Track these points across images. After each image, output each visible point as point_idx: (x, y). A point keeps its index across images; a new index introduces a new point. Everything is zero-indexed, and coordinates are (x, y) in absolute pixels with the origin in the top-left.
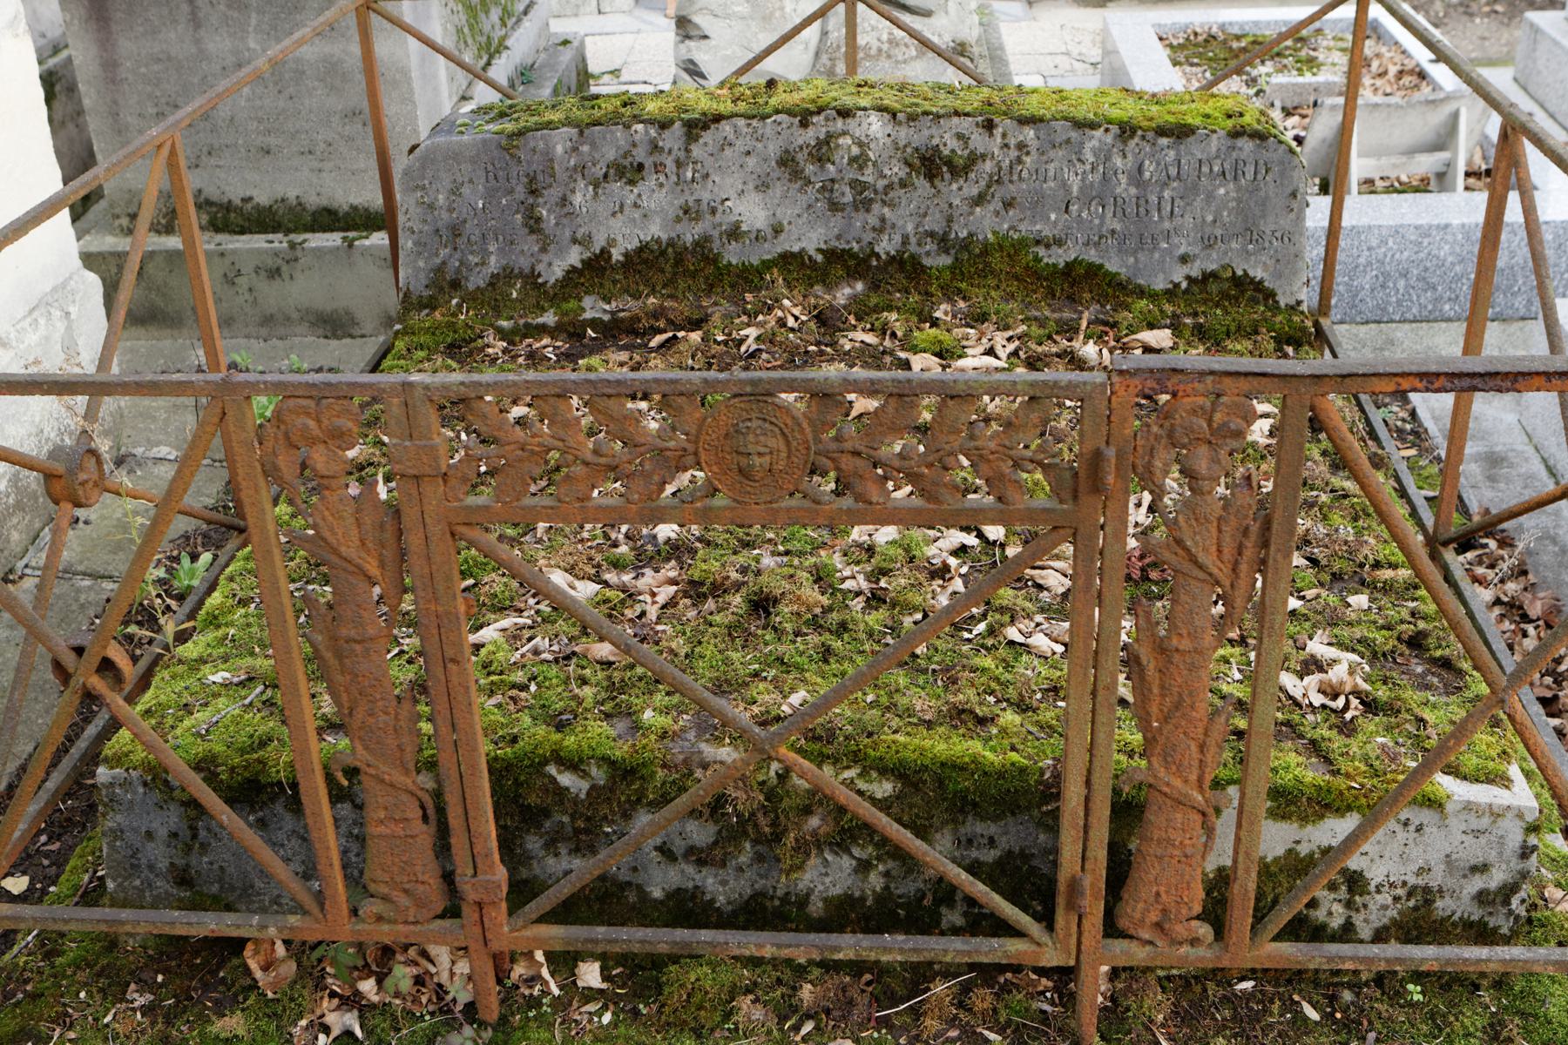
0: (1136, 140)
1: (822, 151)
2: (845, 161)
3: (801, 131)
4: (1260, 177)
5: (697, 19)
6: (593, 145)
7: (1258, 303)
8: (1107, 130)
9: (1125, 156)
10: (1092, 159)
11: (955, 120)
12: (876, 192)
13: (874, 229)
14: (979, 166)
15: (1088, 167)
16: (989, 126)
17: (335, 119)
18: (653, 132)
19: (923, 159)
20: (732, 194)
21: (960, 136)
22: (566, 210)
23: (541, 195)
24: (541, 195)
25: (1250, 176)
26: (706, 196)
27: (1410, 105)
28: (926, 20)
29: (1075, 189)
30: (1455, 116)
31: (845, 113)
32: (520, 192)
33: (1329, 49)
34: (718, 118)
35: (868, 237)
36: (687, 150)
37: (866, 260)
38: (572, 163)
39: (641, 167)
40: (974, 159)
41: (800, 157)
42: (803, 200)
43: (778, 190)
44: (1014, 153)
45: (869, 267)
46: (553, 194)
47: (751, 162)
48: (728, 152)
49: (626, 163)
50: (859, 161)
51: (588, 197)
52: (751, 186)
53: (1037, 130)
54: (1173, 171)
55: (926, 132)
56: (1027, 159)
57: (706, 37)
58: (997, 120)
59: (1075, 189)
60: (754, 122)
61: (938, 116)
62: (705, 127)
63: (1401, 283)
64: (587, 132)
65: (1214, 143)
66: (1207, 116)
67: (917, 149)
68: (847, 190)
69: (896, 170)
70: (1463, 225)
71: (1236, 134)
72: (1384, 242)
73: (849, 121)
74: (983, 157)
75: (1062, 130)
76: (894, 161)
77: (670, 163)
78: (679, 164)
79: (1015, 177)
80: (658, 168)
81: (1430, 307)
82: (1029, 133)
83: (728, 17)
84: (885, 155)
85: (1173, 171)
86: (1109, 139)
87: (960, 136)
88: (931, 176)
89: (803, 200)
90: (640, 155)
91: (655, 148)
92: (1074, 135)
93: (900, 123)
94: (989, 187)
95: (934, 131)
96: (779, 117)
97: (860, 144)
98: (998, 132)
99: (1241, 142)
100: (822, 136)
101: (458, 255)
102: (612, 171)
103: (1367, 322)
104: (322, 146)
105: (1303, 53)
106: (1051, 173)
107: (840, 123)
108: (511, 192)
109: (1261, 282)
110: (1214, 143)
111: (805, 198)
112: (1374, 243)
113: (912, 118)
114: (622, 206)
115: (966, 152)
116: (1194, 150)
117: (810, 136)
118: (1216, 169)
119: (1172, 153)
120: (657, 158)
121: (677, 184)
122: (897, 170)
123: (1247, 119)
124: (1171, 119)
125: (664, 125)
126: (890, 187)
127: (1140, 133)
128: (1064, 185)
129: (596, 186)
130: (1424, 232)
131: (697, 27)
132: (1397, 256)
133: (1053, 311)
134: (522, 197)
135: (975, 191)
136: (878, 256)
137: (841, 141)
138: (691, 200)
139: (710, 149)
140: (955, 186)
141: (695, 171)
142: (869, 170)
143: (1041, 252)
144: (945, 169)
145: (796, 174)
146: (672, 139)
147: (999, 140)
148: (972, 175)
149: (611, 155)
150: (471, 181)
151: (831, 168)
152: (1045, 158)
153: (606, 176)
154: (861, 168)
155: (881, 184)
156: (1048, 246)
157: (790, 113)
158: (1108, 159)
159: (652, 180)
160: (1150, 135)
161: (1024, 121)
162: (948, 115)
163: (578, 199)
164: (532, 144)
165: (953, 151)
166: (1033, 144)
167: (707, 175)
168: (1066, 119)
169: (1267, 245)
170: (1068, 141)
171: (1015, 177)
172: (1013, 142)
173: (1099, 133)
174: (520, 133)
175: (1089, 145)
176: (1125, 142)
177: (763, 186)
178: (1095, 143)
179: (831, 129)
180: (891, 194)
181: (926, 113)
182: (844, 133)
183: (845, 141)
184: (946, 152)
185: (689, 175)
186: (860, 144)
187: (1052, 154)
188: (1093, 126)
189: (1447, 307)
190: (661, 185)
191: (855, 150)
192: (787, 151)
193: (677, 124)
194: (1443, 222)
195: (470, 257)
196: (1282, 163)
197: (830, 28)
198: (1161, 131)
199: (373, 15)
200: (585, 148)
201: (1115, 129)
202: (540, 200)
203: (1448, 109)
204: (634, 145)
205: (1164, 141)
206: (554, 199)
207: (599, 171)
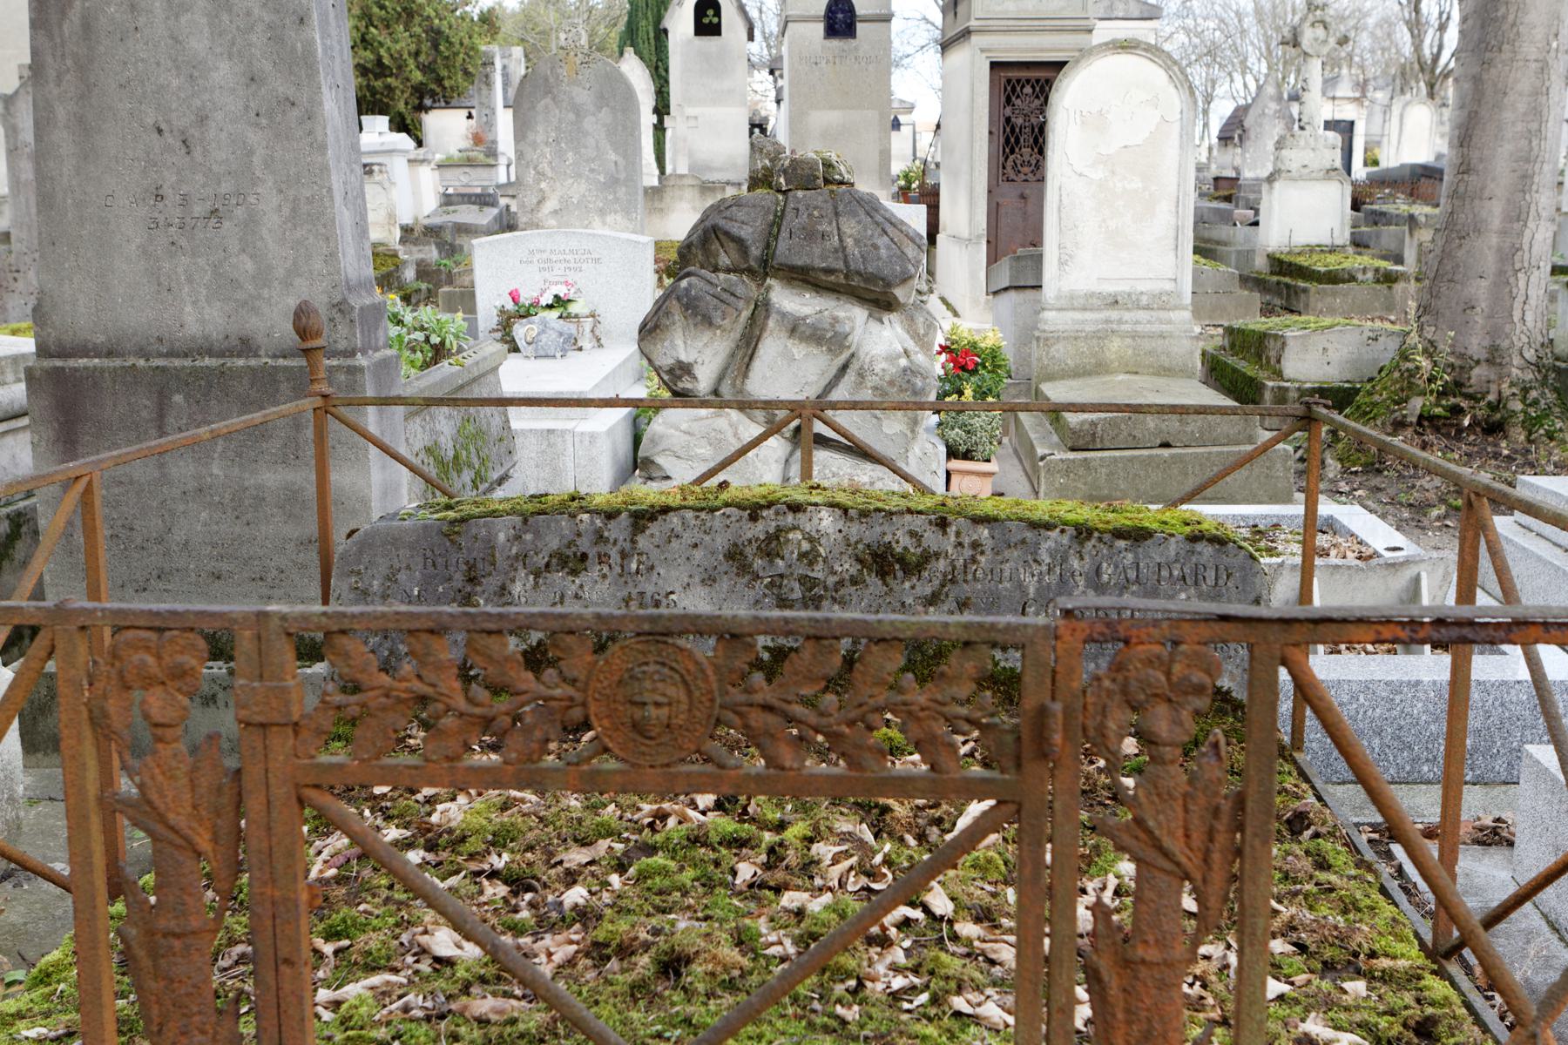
0: (1093, 541)
1: (771, 546)
2: (795, 556)
3: (750, 525)
4: (1221, 582)
5: (660, 460)
6: (537, 534)
7: (1226, 714)
8: (1063, 531)
9: (1082, 558)
10: (1048, 560)
11: (908, 517)
12: (826, 588)
14: (933, 564)
15: (1045, 568)
16: (943, 524)
17: (290, 547)
18: (598, 522)
19: (875, 555)
20: (678, 587)
21: (912, 534)
22: (504, 599)
23: (480, 584)
24: (480, 584)
25: (1211, 581)
26: (650, 589)
27: (1372, 569)
29: (1032, 590)
30: (1417, 580)
31: (796, 508)
32: (459, 579)
33: (1287, 541)
34: (666, 510)
36: (633, 542)
38: (514, 551)
39: (584, 557)
40: (927, 557)
41: (749, 551)
42: (751, 595)
43: (724, 584)
44: (968, 553)
46: (492, 583)
47: (698, 554)
48: (675, 544)
49: (569, 552)
50: (809, 557)
51: (528, 586)
52: (697, 579)
53: (991, 529)
54: (1132, 575)
55: (878, 529)
56: (982, 559)
57: (668, 478)
58: (950, 518)
59: (1032, 590)
60: (703, 515)
61: (892, 513)
62: (653, 518)
63: (1377, 741)
64: (531, 520)
65: (1173, 547)
66: (1165, 523)
67: (869, 546)
68: (797, 585)
69: (847, 566)
70: (1435, 683)
71: (1194, 538)
72: (1354, 698)
73: (799, 515)
74: (937, 555)
75: (1018, 532)
76: (845, 557)
77: (614, 553)
78: (624, 555)
79: (970, 577)
80: (603, 558)
81: (1408, 768)
82: (984, 532)
83: (690, 458)
84: (836, 551)
85: (1132, 575)
86: (1065, 540)
87: (912, 534)
88: (883, 574)
89: (751, 595)
90: (584, 545)
91: (600, 538)
92: (1029, 535)
93: (852, 520)
94: (943, 586)
95: (886, 527)
96: (728, 511)
97: (811, 540)
98: (952, 530)
99: (1199, 547)
100: (772, 530)
101: (387, 644)
102: (554, 561)
103: (1344, 783)
104: (275, 572)
105: (1262, 544)
106: (1007, 574)
107: (790, 518)
108: (450, 579)
109: (1228, 692)
110: (1173, 547)
111: (752, 593)
112: (1345, 698)
113: (864, 514)
114: (562, 597)
115: (919, 550)
116: (1153, 554)
117: (759, 530)
118: (1176, 573)
119: (1130, 556)
120: (602, 548)
121: (621, 576)
122: (848, 567)
123: (1205, 526)
124: (1128, 523)
125: (611, 515)
126: (841, 583)
127: (1096, 534)
128: (1020, 586)
129: (537, 575)
130: (1396, 688)
131: (660, 468)
132: (1370, 713)
133: (1011, 716)
134: (460, 586)
135: (928, 590)
137: (791, 536)
138: (634, 592)
139: (656, 541)
140: (907, 585)
141: (640, 562)
142: (819, 566)
143: (998, 655)
144: (897, 567)
145: (744, 568)
146: (618, 530)
147: (953, 538)
148: (925, 574)
149: (554, 543)
150: (408, 567)
151: (780, 563)
152: (999, 558)
153: (547, 565)
154: (811, 564)
155: (832, 580)
156: (1004, 649)
157: (740, 507)
158: (1064, 560)
159: (594, 571)
160: (1107, 537)
161: (979, 520)
162: (901, 513)
163: (517, 589)
164: (474, 531)
165: (905, 548)
166: (988, 544)
167: (652, 568)
168: (1021, 520)
169: (1232, 653)
170: (1023, 541)
171: (970, 577)
172: (966, 541)
173: (1055, 534)
174: (463, 520)
175: (1045, 546)
176: (1081, 544)
177: (709, 580)
178: (1050, 544)
179: (782, 523)
180: (842, 592)
181: (878, 510)
182: (795, 528)
183: (795, 536)
184: (899, 550)
185: (634, 566)
186: (811, 540)
187: (1007, 554)
188: (1048, 526)
189: (1426, 768)
190: (604, 576)
191: (806, 546)
192: (735, 545)
193: (624, 515)
194: (1414, 679)
195: (401, 647)
196: (1243, 568)
198: (1119, 534)
200: (528, 537)
201: (1071, 531)
202: (478, 589)
203: (1409, 573)
204: (579, 535)
205: (1121, 544)
206: (492, 589)
207: (541, 560)
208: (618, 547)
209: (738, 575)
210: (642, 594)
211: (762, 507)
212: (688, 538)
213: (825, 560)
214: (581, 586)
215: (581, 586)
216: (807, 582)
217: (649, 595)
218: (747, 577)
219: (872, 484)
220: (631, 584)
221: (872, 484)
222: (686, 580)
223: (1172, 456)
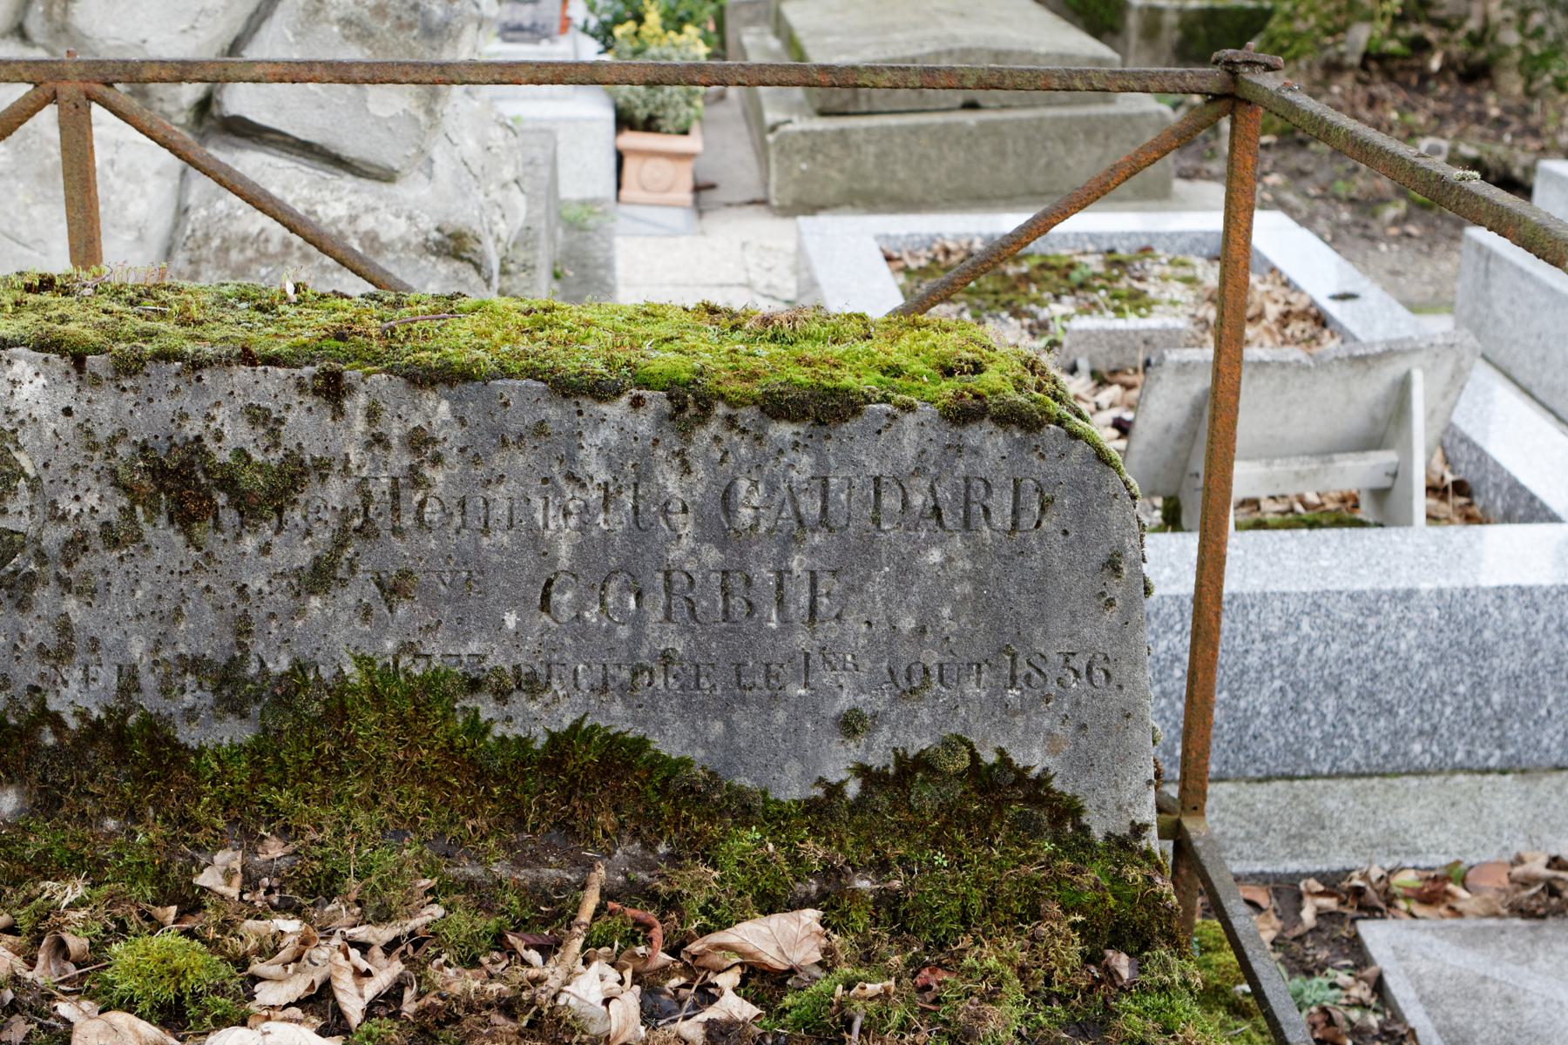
0: (714, 427)
4: (1027, 521)
7: (1037, 833)
8: (637, 403)
9: (686, 469)
10: (602, 476)
11: (242, 373)
12: (41, 557)
13: (42, 651)
14: (312, 491)
15: (595, 495)
16: (332, 389)
19: (158, 471)
21: (256, 416)
25: (1001, 519)
27: (1322, 365)
28: (385, 188)
29: (564, 551)
30: (1404, 385)
33: (1164, 279)
35: (28, 672)
37: (27, 732)
40: (294, 476)
44: (400, 460)
45: (35, 748)
53: (456, 401)
54: (811, 507)
55: (166, 405)
56: (437, 475)
58: (351, 374)
59: (564, 551)
61: (197, 365)
63: (1329, 704)
65: (910, 437)
66: (895, 371)
67: (144, 448)
69: (91, 500)
70: (1440, 593)
71: (962, 414)
72: (1292, 625)
74: (322, 468)
75: (524, 403)
76: (86, 478)
79: (408, 521)
81: (1385, 748)
82: (438, 409)
84: (61, 464)
85: (811, 507)
86: (644, 424)
87: (256, 416)
88: (184, 519)
92: (553, 412)
93: (96, 381)
94: (341, 546)
95: (186, 401)
98: (356, 405)
99: (974, 435)
103: (1268, 779)
105: (1123, 285)
106: (500, 511)
109: (1042, 780)
110: (910, 437)
112: (1275, 626)
113: (128, 367)
115: (275, 457)
116: (861, 453)
118: (917, 500)
119: (805, 461)
122: (95, 502)
123: (991, 378)
124: (802, 376)
126: (77, 545)
127: (721, 409)
128: (536, 541)
130: (1367, 604)
132: (1319, 651)
133: (518, 863)
135: (304, 556)
136: (56, 721)
140: (250, 543)
143: (487, 708)
144: (221, 499)
147: (360, 425)
148: (295, 515)
152: (481, 471)
155: (54, 536)
156: (502, 695)
158: (643, 474)
160: (748, 415)
161: (423, 378)
162: (223, 362)
165: (241, 453)
166: (451, 438)
168: (532, 373)
169: (1053, 688)
170: (540, 429)
171: (408, 521)
172: (396, 431)
173: (616, 410)
175: (593, 440)
176: (685, 433)
178: (607, 434)
180: (84, 563)
181: (165, 356)
184: (224, 457)
187: (499, 461)
188: (602, 391)
189: (1417, 748)
194: (1402, 585)
196: (1078, 486)
197: (191, 200)
198: (777, 406)
201: (657, 401)
203: (1390, 373)
205: (783, 431)
213: (35, 485)
219: (353, 219)
221: (353, 219)
223: (982, 125)
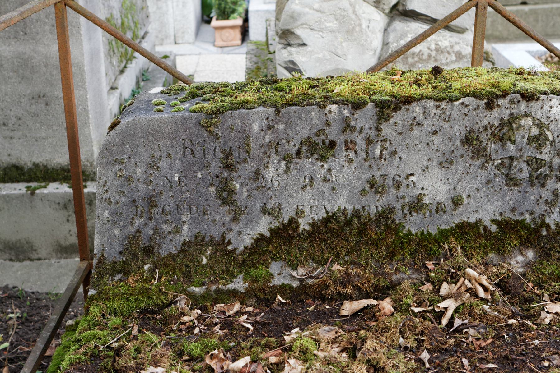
1: (504, 132)
2: (525, 140)
3: (486, 112)
5: (298, 32)
6: (289, 124)
13: (547, 202)
17: (24, 101)
18: (346, 113)
20: (417, 170)
22: (258, 183)
23: (236, 170)
24: (236, 170)
26: (392, 172)
28: (460, 35)
31: (528, 97)
32: (216, 166)
34: (408, 100)
35: (540, 209)
36: (378, 129)
37: (537, 231)
38: (267, 140)
39: (332, 144)
41: (483, 136)
42: (483, 175)
43: (460, 166)
45: (541, 236)
46: (246, 169)
47: (437, 140)
48: (416, 131)
49: (319, 140)
50: (538, 141)
51: (281, 171)
52: (435, 162)
57: (304, 45)
60: (443, 104)
62: (397, 108)
64: (283, 111)
68: (525, 167)
73: (532, 104)
77: (360, 142)
78: (369, 141)
80: (349, 145)
83: (321, 30)
89: (483, 175)
90: (333, 133)
91: (347, 127)
96: (466, 100)
97: (540, 125)
100: (506, 118)
101: (152, 224)
102: (304, 148)
104: (14, 120)
107: (523, 106)
108: (207, 166)
111: (484, 173)
114: (312, 180)
117: (494, 117)
120: (348, 136)
121: (366, 160)
125: (357, 106)
129: (288, 162)
131: (297, 37)
134: (217, 171)
136: (548, 227)
137: (523, 122)
138: (377, 175)
139: (399, 128)
141: (383, 148)
142: (547, 149)
145: (479, 152)
146: (364, 119)
149: (305, 133)
150: (169, 156)
151: (512, 147)
153: (299, 153)
154: (540, 146)
157: (479, 97)
159: (341, 157)
163: (270, 173)
164: (230, 122)
167: (395, 152)
174: (219, 112)
177: (447, 163)
179: (515, 111)
182: (527, 115)
183: (527, 122)
185: (378, 152)
186: (540, 125)
190: (350, 161)
191: (535, 131)
192: (471, 131)
193: (370, 105)
195: (164, 226)
197: (390, 40)
199: (69, 10)
200: (281, 127)
202: (235, 174)
204: (328, 124)
206: (247, 174)
207: (292, 149)
208: (364, 135)
209: (472, 158)
210: (384, 176)
211: (497, 97)
212: (428, 125)
213: (552, 143)
214: (329, 170)
215: (329, 170)
216: (535, 163)
217: (391, 176)
218: (481, 160)
219: (452, 47)
220: (375, 168)
221: (452, 47)
222: (425, 163)
223: (531, 10)
